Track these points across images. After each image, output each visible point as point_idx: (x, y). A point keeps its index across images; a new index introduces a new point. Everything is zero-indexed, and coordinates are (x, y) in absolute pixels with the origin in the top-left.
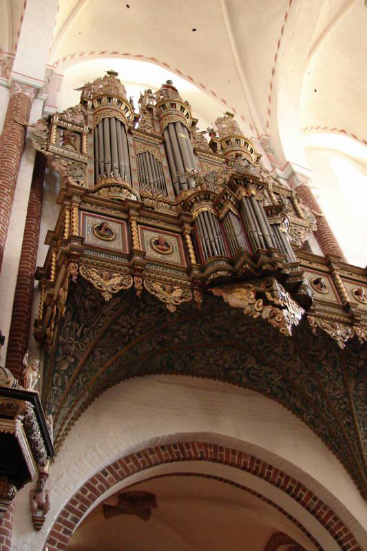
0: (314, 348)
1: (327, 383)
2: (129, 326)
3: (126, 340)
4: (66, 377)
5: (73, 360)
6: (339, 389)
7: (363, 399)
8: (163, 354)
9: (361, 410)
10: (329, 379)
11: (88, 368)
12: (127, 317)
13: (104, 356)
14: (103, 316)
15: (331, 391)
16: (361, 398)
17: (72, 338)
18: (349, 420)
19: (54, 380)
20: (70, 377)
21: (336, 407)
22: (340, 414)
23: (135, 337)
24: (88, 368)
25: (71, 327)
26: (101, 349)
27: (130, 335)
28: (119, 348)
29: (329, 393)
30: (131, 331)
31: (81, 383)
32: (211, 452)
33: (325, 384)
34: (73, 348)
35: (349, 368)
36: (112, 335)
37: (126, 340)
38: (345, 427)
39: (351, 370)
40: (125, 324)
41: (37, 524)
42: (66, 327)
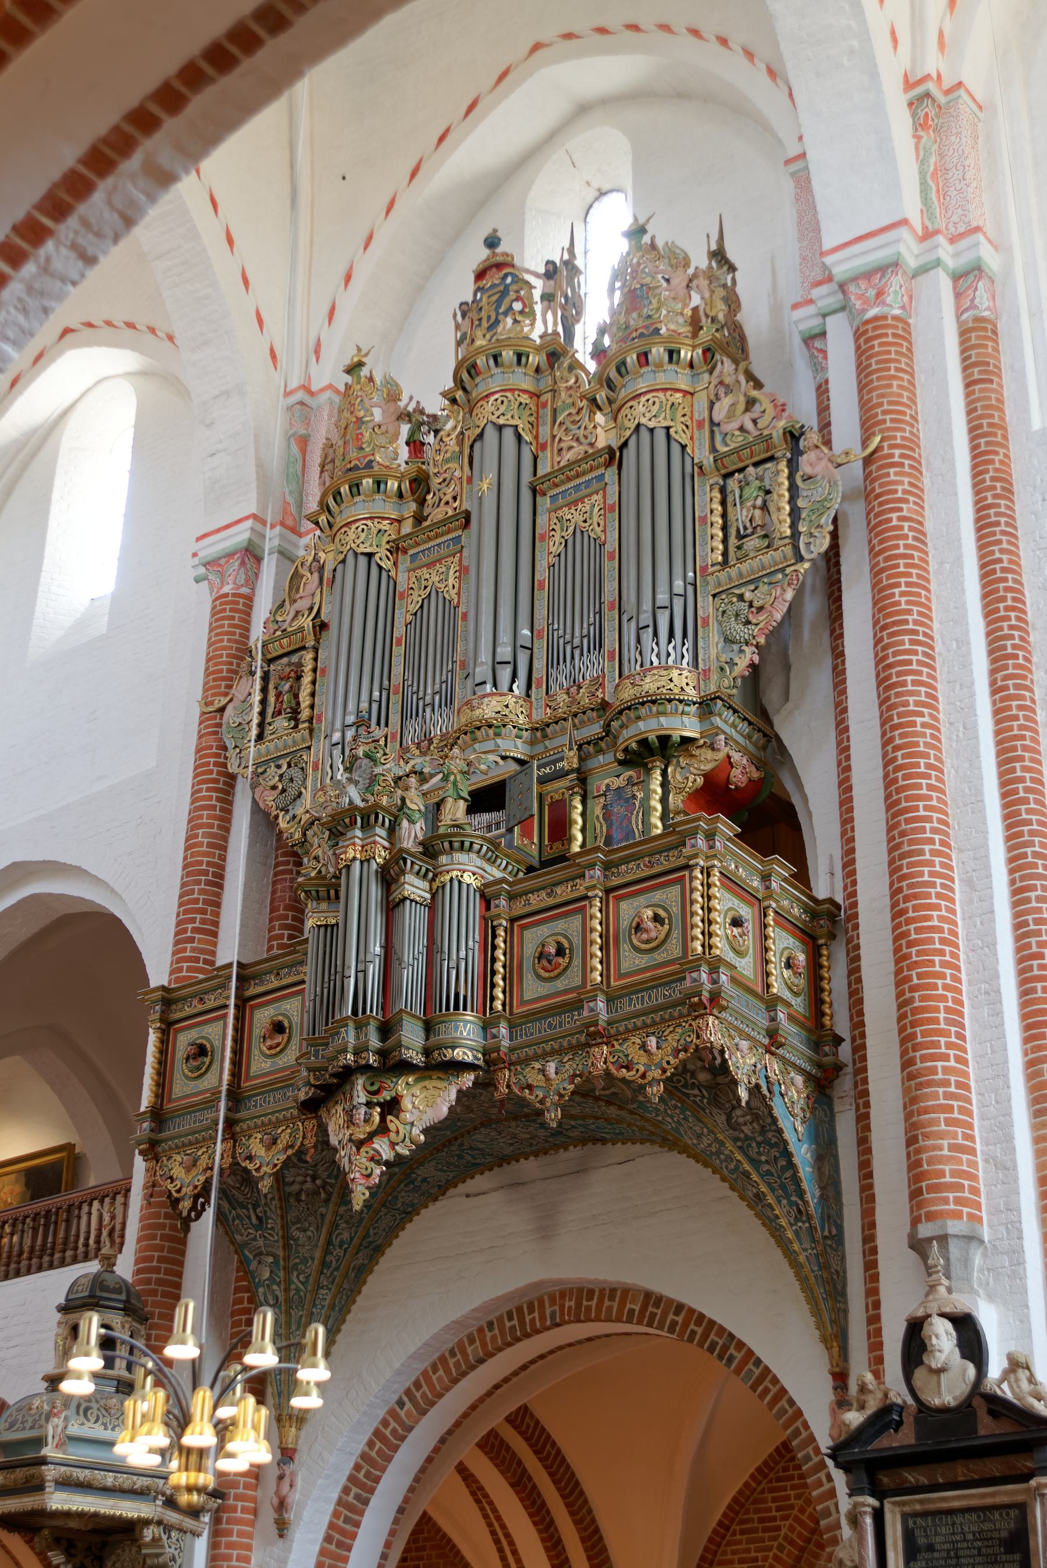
2: (309, 1179)
4: (275, 1287)
5: (271, 1259)
7: (760, 1139)
9: (767, 1162)
13: (309, 1233)
16: (754, 1139)
23: (332, 1186)
27: (323, 1187)
28: (323, 1210)
30: (318, 1182)
32: (570, 1308)
34: (261, 1242)
35: (687, 1095)
36: (299, 1201)
37: (323, 1195)
40: (300, 1179)
41: (282, 1527)
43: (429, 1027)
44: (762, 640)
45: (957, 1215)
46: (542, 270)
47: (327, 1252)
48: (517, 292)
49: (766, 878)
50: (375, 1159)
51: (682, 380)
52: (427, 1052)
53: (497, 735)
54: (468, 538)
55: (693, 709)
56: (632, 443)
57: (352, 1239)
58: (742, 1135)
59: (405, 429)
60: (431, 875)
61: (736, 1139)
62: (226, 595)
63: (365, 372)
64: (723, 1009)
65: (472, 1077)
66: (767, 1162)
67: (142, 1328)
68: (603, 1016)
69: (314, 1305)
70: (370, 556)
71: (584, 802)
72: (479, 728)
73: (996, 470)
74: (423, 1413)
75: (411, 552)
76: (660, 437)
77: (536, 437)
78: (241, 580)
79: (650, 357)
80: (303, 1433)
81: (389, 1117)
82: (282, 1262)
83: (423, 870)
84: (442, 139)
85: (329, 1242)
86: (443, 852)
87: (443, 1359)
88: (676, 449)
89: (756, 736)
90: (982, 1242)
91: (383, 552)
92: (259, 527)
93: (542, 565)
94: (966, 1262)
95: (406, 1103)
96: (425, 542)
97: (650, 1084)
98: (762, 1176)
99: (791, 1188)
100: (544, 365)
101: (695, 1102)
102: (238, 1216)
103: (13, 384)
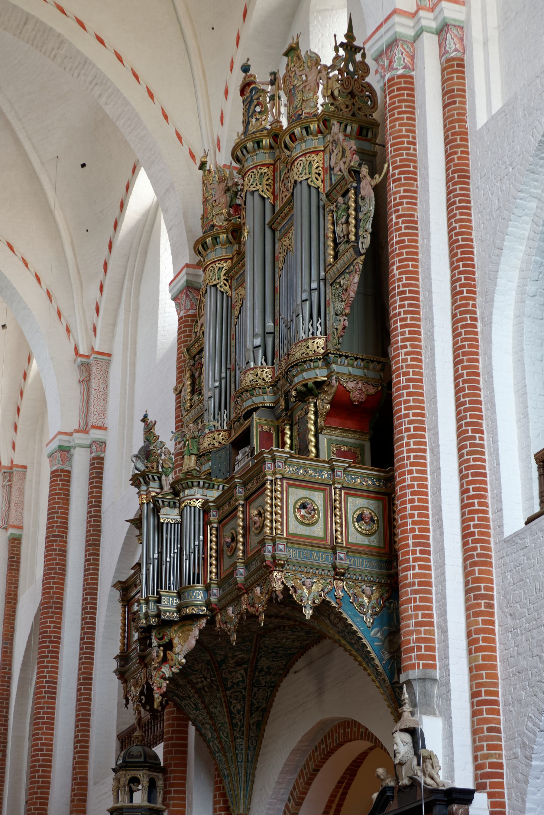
3: (215, 687)
13: (218, 709)
30: (208, 680)
37: (215, 687)
43: (179, 595)
44: (347, 311)
45: (413, 666)
46: (268, 78)
48: (258, 99)
49: (333, 470)
50: (163, 678)
51: (316, 143)
52: (179, 609)
53: (252, 395)
55: (320, 363)
57: (244, 708)
60: (177, 505)
64: (282, 566)
65: (205, 621)
67: (160, 776)
68: (240, 579)
70: (215, 286)
71: (291, 430)
72: (242, 393)
73: (455, 165)
74: (300, 804)
81: (168, 652)
83: (172, 503)
87: (302, 771)
89: (371, 366)
90: (435, 680)
91: (222, 281)
92: (191, 271)
94: (425, 694)
95: (176, 641)
96: (240, 271)
100: (273, 144)
102: (186, 705)
103: (127, 189)
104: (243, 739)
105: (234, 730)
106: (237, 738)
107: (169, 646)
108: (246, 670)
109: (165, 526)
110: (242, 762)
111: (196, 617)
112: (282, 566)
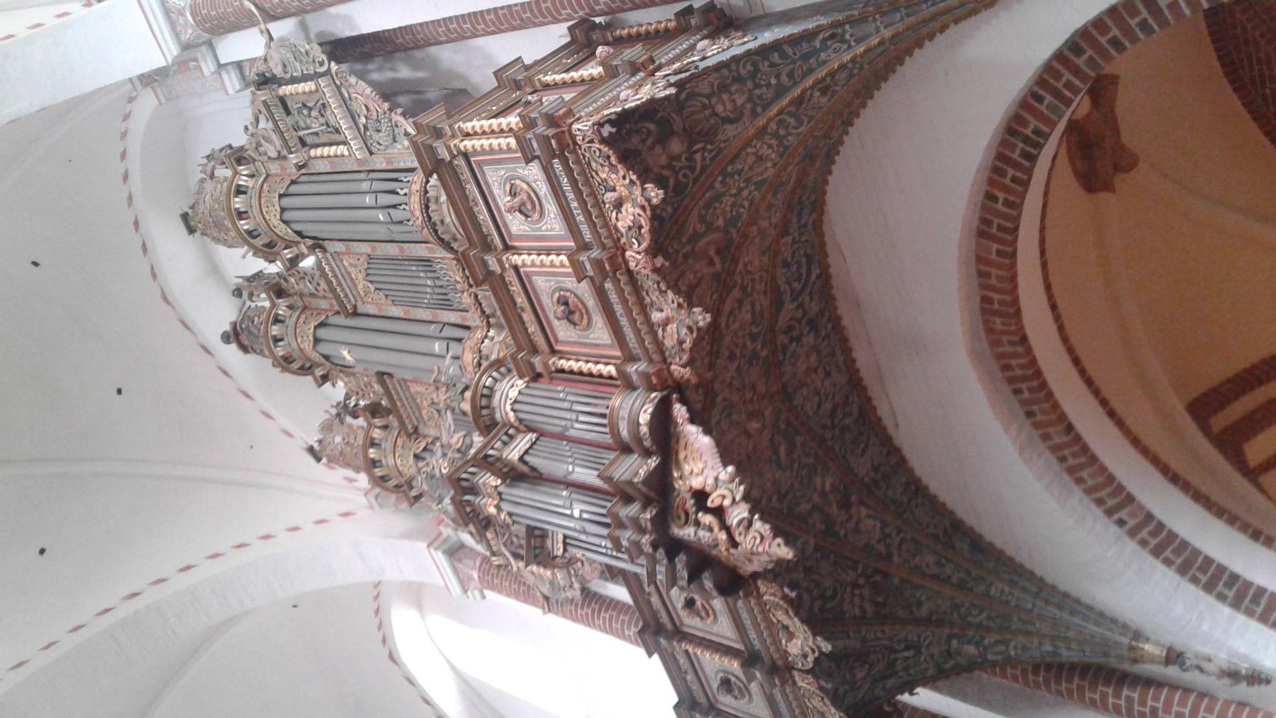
0: (706, 270)
1: (755, 184)
2: (857, 592)
3: (878, 578)
4: (986, 641)
6: (756, 154)
7: (750, 84)
8: (856, 471)
9: (778, 76)
10: (747, 187)
11: (955, 615)
12: (846, 607)
13: (923, 598)
14: (864, 640)
15: (769, 164)
16: (750, 91)
17: (922, 659)
18: (817, 94)
19: (1000, 657)
20: (983, 638)
21: (798, 134)
22: (811, 118)
24: (955, 615)
25: (906, 669)
26: (914, 609)
28: (896, 581)
29: (775, 165)
30: (861, 581)
31: (984, 615)
33: (758, 185)
35: (704, 168)
36: (884, 604)
37: (878, 578)
38: (835, 92)
39: (704, 158)
40: (857, 600)
42: (910, 675)
47: (947, 580)
52: (647, 454)
54: (399, 374)
56: (298, 227)
58: (748, 106)
59: (349, 419)
60: (511, 431)
61: (754, 114)
62: (479, 577)
63: (316, 446)
64: (570, 113)
66: (778, 76)
69: (1007, 602)
75: (416, 423)
76: (287, 202)
77: (326, 311)
78: (470, 563)
79: (243, 210)
80: (1152, 636)
81: (709, 504)
82: (956, 631)
83: (505, 438)
84: (225, 373)
85: (935, 577)
86: (492, 416)
88: (293, 189)
92: (436, 544)
93: (396, 311)
95: (696, 483)
97: (649, 200)
98: (795, 84)
99: (805, 47)
101: (712, 160)
104: (991, 584)
105: (971, 590)
106: (988, 592)
107: (701, 496)
108: (861, 502)
109: (527, 458)
110: (1034, 605)
111: (662, 417)
112: (570, 113)
